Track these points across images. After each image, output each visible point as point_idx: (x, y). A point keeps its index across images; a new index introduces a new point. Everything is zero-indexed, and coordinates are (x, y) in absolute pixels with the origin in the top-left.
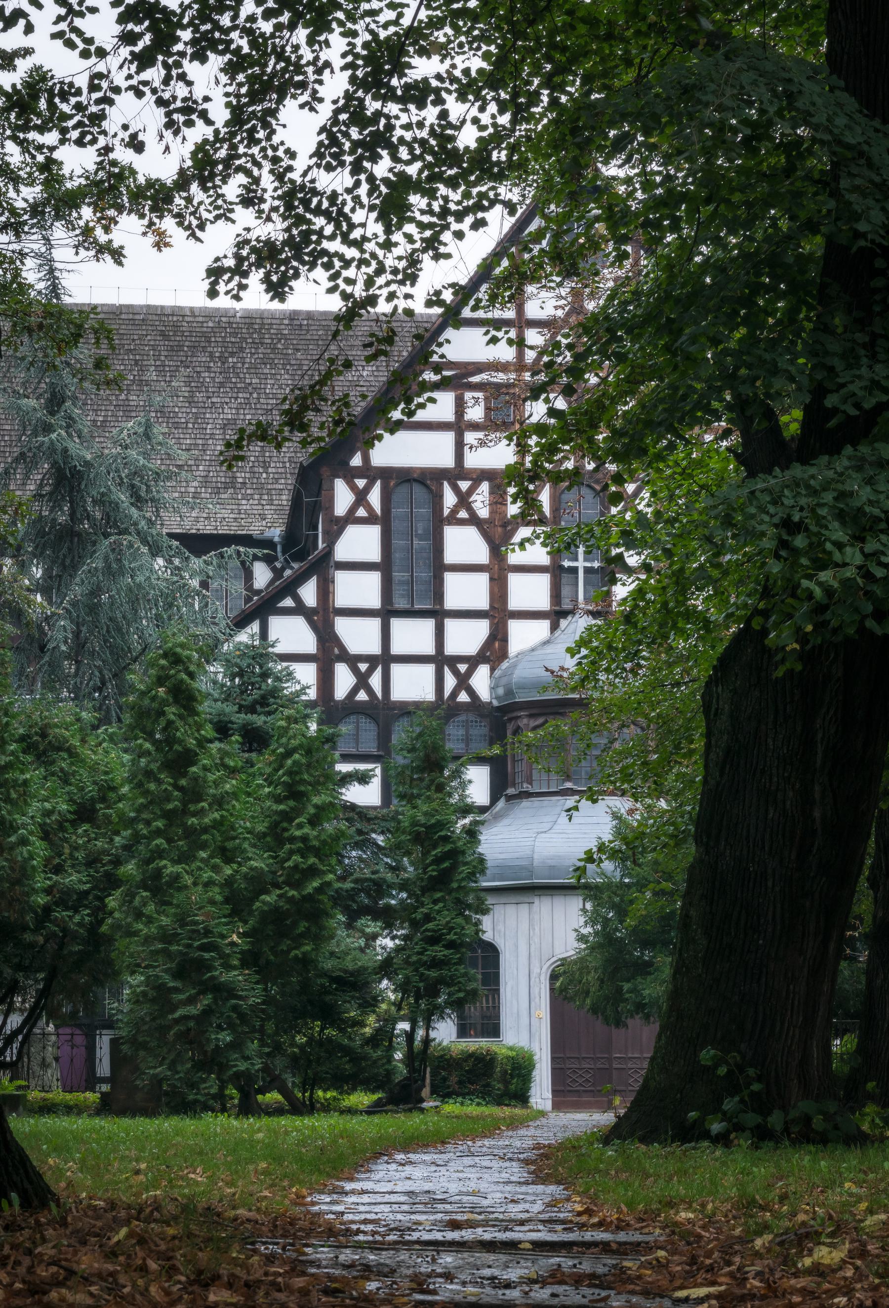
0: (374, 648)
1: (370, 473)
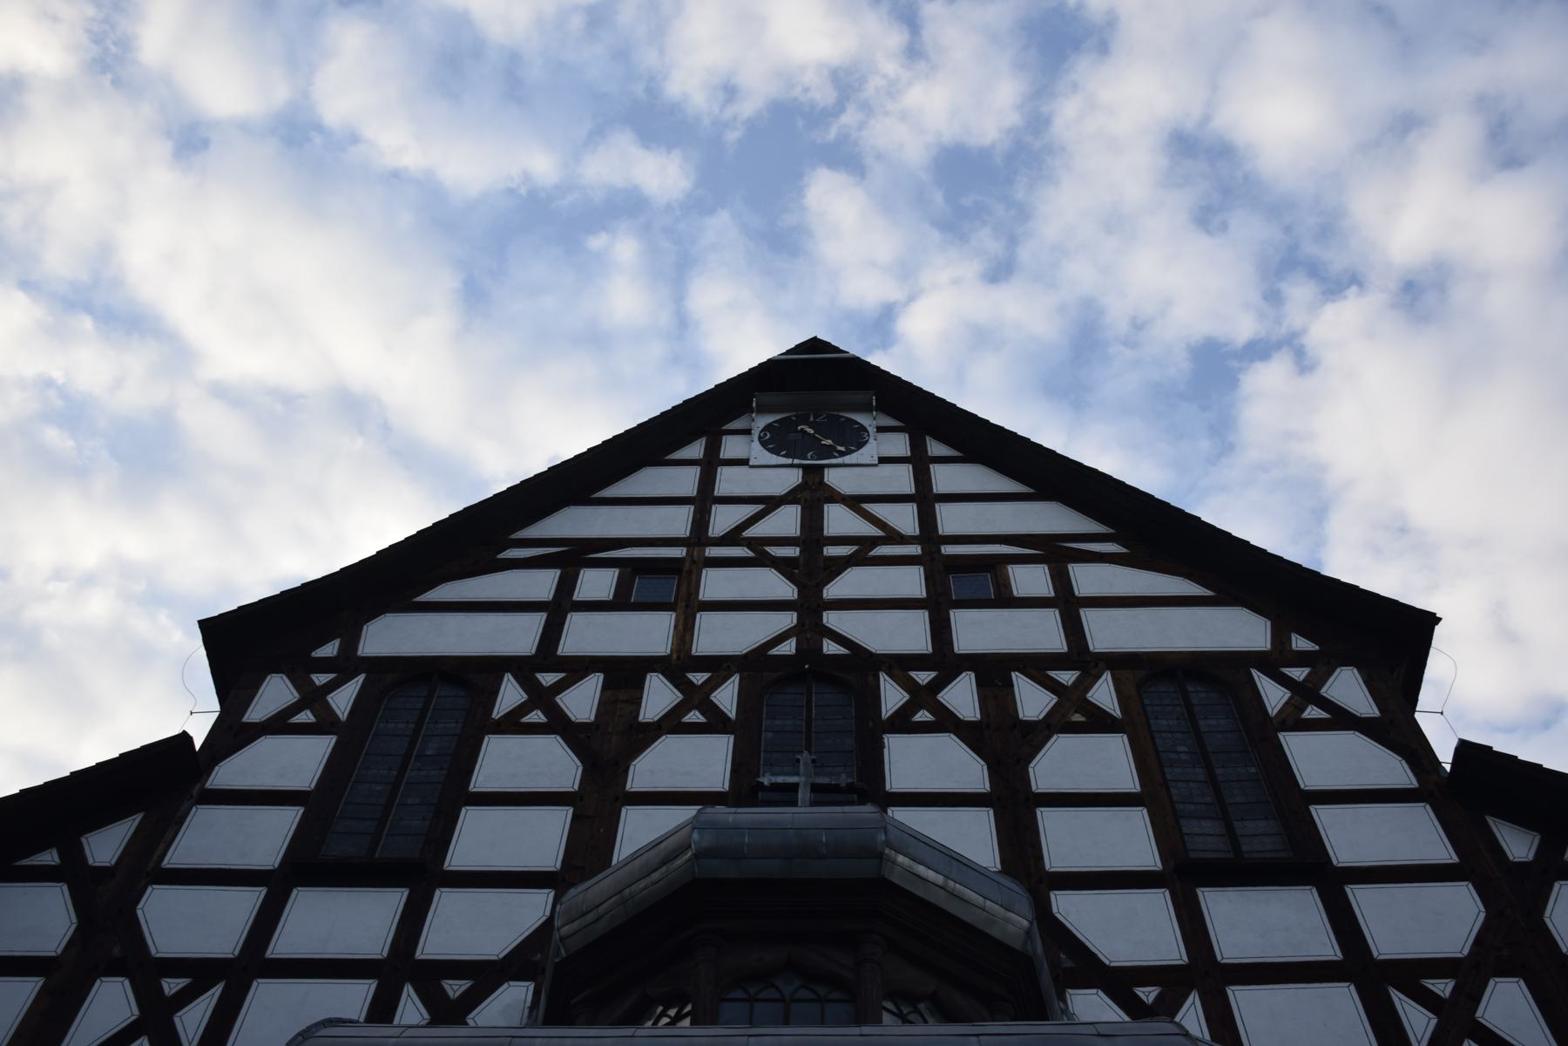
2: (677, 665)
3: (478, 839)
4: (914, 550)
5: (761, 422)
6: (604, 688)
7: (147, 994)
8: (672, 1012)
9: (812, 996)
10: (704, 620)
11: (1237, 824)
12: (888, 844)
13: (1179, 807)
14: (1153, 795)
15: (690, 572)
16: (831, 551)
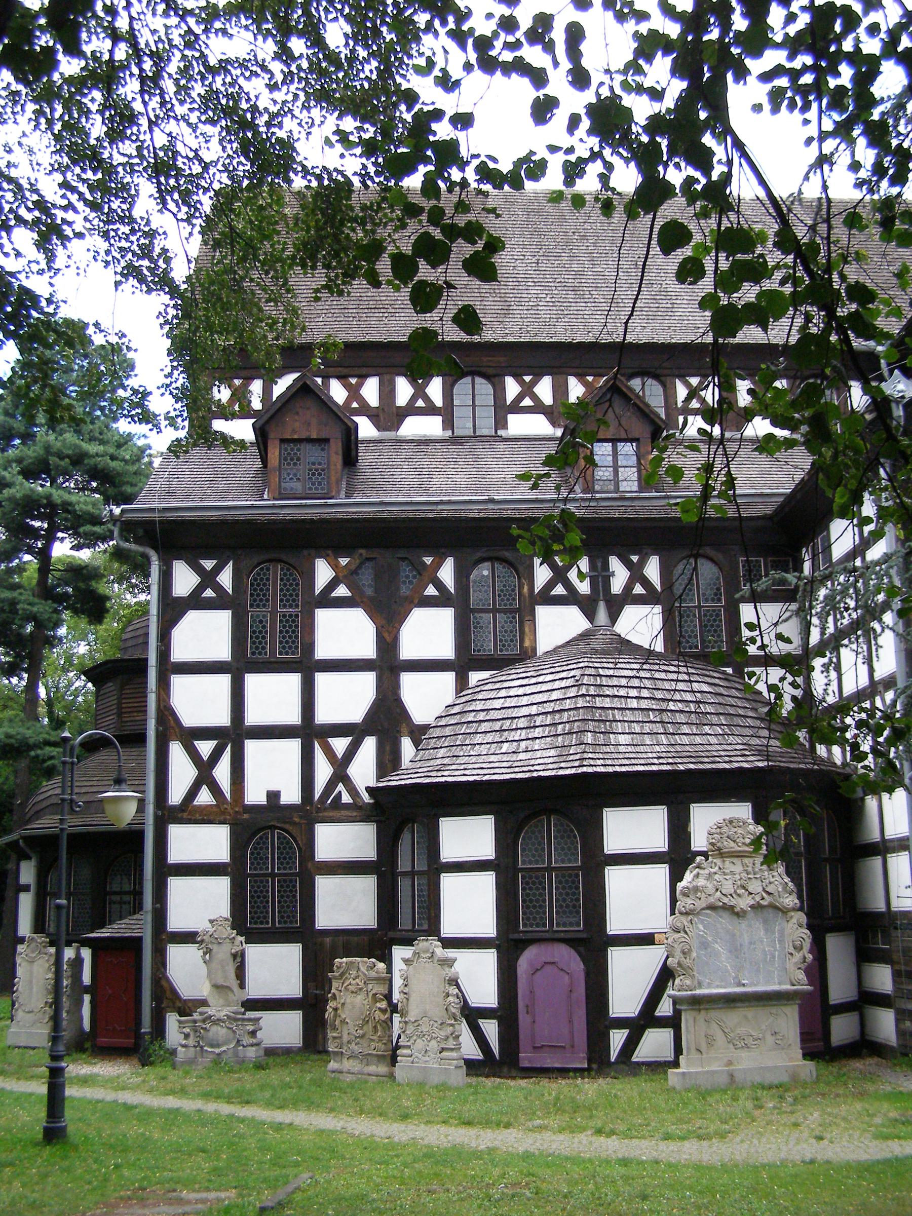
0: (222, 717)
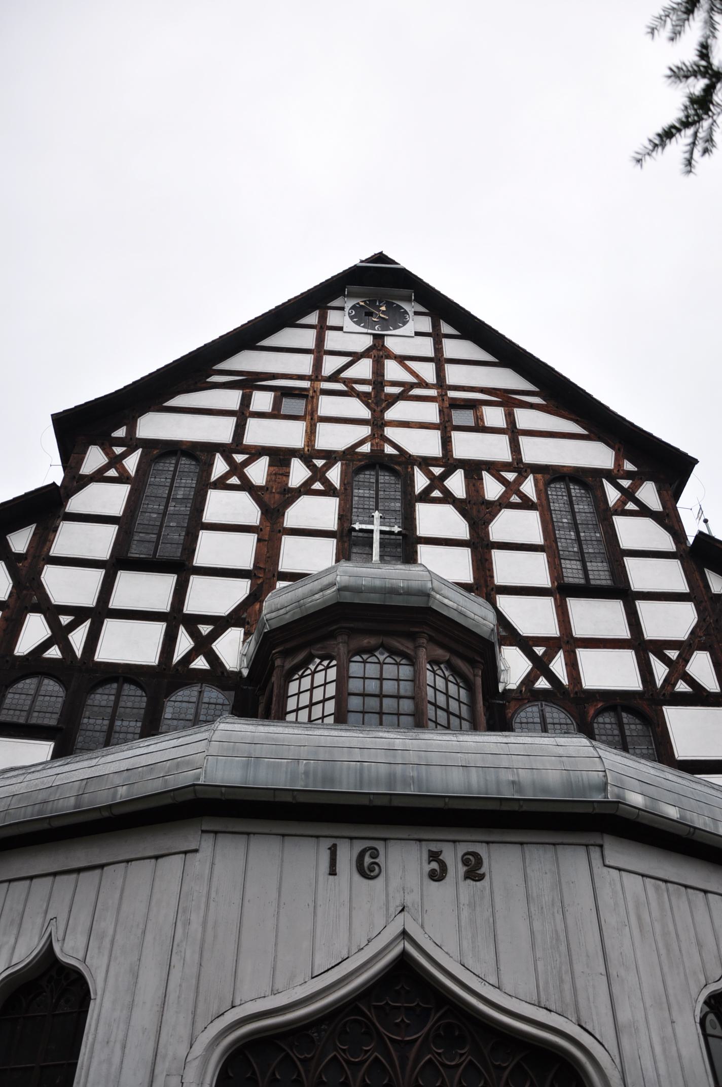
1: (132, 443)
2: (308, 455)
3: (210, 549)
4: (433, 392)
5: (349, 304)
6: (270, 465)
7: (53, 623)
8: (325, 663)
9: (393, 662)
10: (322, 429)
11: (588, 564)
12: (433, 589)
13: (561, 553)
14: (549, 547)
15: (312, 397)
16: (389, 390)
